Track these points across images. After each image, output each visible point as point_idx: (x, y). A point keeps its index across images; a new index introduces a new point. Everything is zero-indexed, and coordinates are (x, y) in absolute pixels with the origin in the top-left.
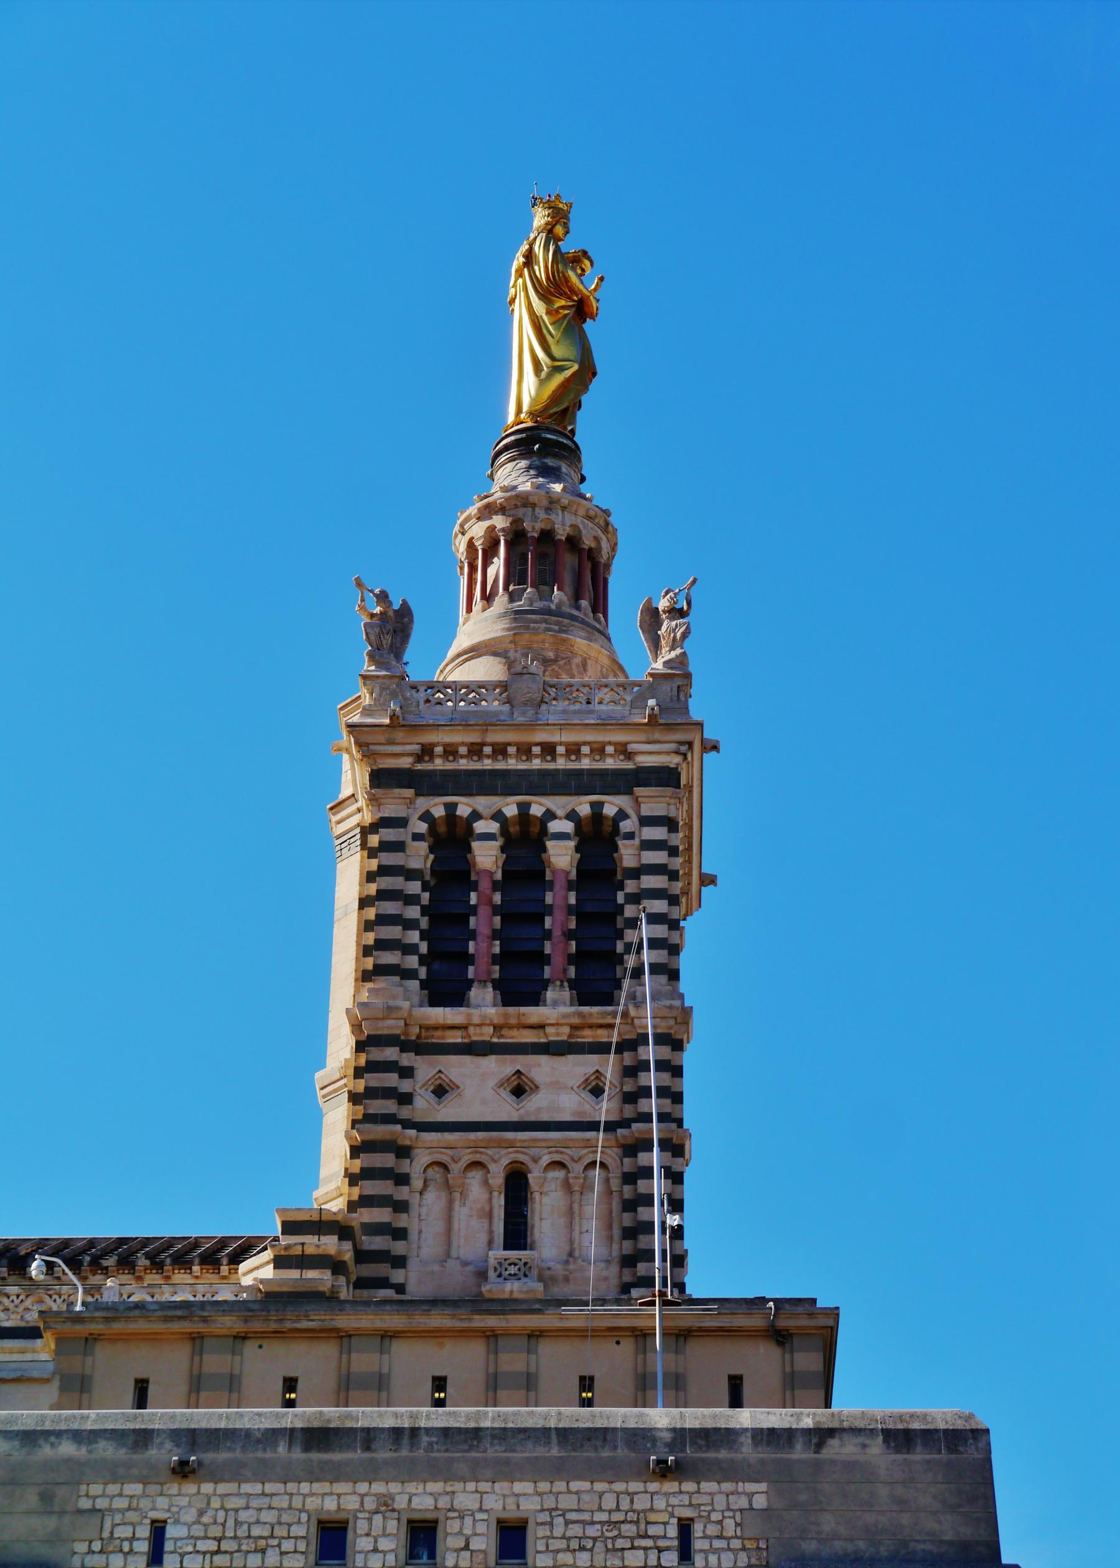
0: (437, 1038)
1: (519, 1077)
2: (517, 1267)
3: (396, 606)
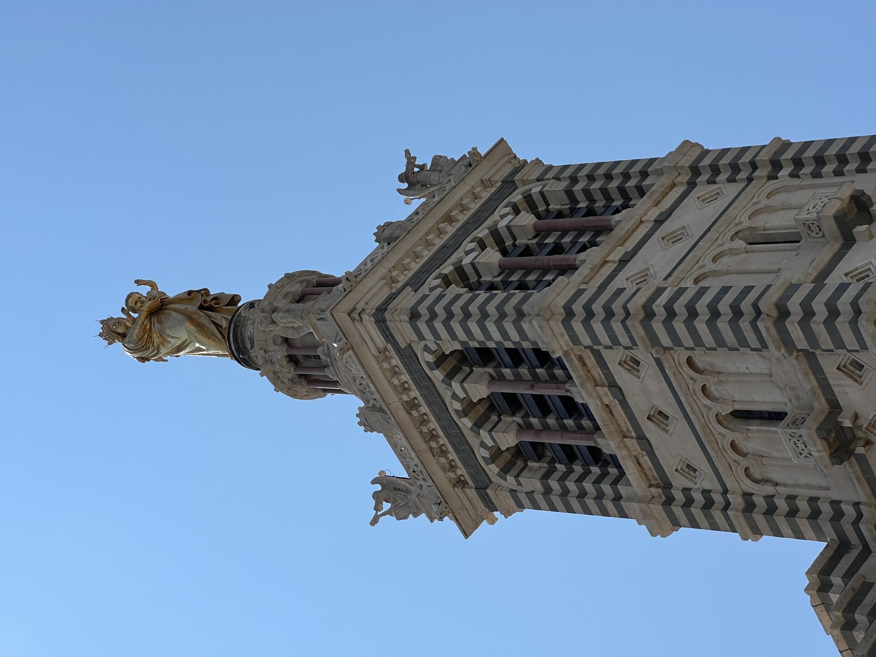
0: (653, 473)
1: (653, 416)
2: (797, 442)
3: (378, 487)
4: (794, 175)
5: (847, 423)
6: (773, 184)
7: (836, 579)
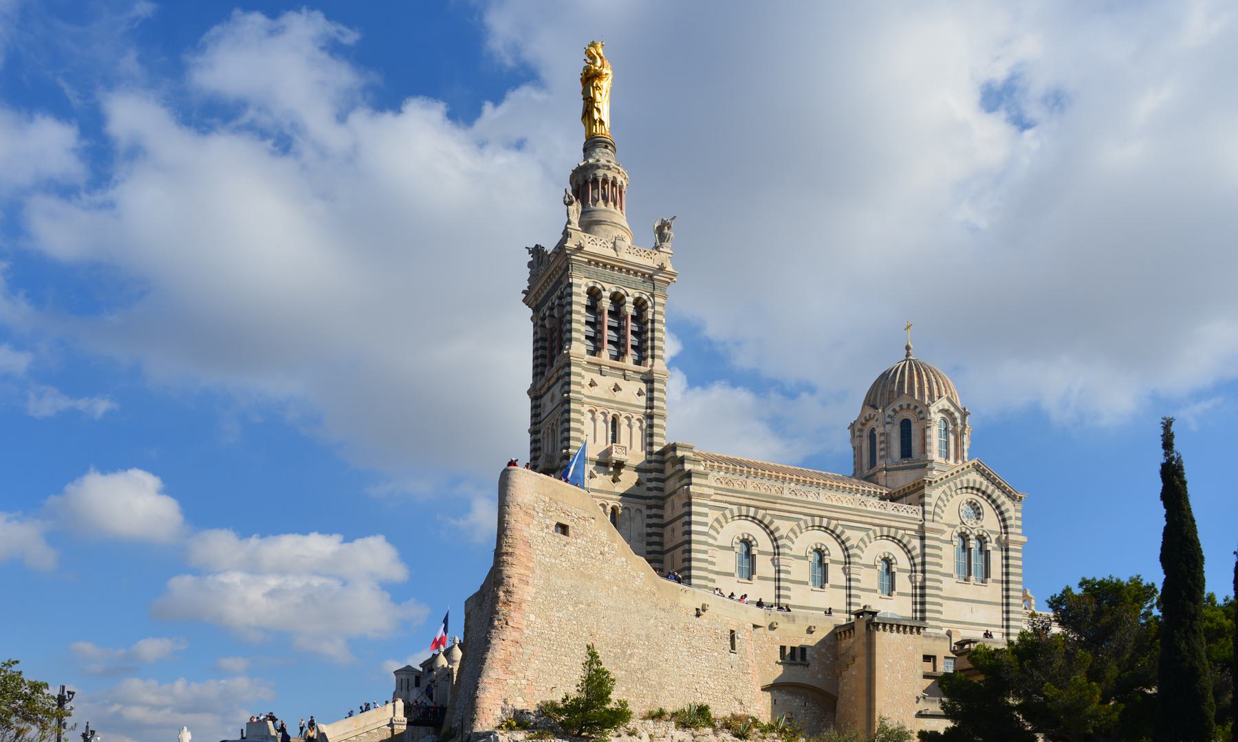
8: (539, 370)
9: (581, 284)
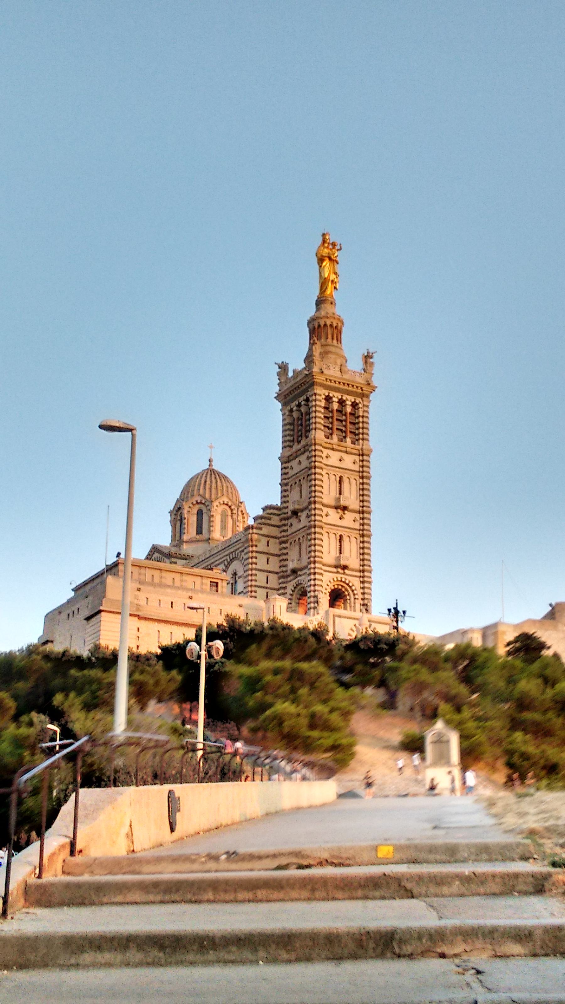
4: (360, 483)
5: (299, 514)
6: (358, 478)
7: (272, 511)
8: (288, 443)
9: (321, 392)
